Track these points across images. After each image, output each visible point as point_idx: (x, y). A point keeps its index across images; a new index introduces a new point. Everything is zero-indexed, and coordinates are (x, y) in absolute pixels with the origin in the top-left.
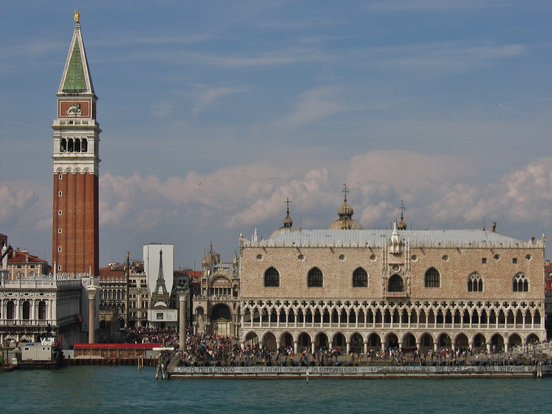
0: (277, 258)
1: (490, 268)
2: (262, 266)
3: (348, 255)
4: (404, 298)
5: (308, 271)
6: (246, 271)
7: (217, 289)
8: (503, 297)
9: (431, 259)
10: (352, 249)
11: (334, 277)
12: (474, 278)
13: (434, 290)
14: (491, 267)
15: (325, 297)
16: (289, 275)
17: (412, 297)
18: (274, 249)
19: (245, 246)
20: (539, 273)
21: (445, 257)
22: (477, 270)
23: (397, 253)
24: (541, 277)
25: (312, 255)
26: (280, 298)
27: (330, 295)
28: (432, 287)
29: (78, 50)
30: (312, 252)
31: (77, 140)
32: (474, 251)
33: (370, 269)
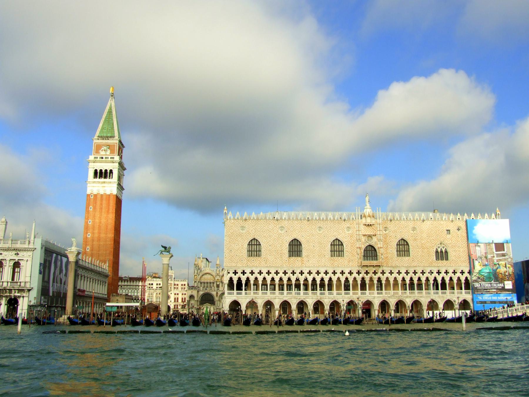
0: (259, 230)
1: (453, 239)
2: (245, 237)
4: (379, 266)
5: (287, 242)
6: (230, 242)
7: (204, 283)
9: (401, 230)
10: (329, 221)
13: (405, 259)
16: (270, 246)
17: (385, 265)
18: (256, 222)
19: (228, 218)
21: (414, 229)
23: (371, 225)
25: (292, 227)
26: (262, 267)
30: (292, 224)
31: (106, 170)
33: (346, 240)
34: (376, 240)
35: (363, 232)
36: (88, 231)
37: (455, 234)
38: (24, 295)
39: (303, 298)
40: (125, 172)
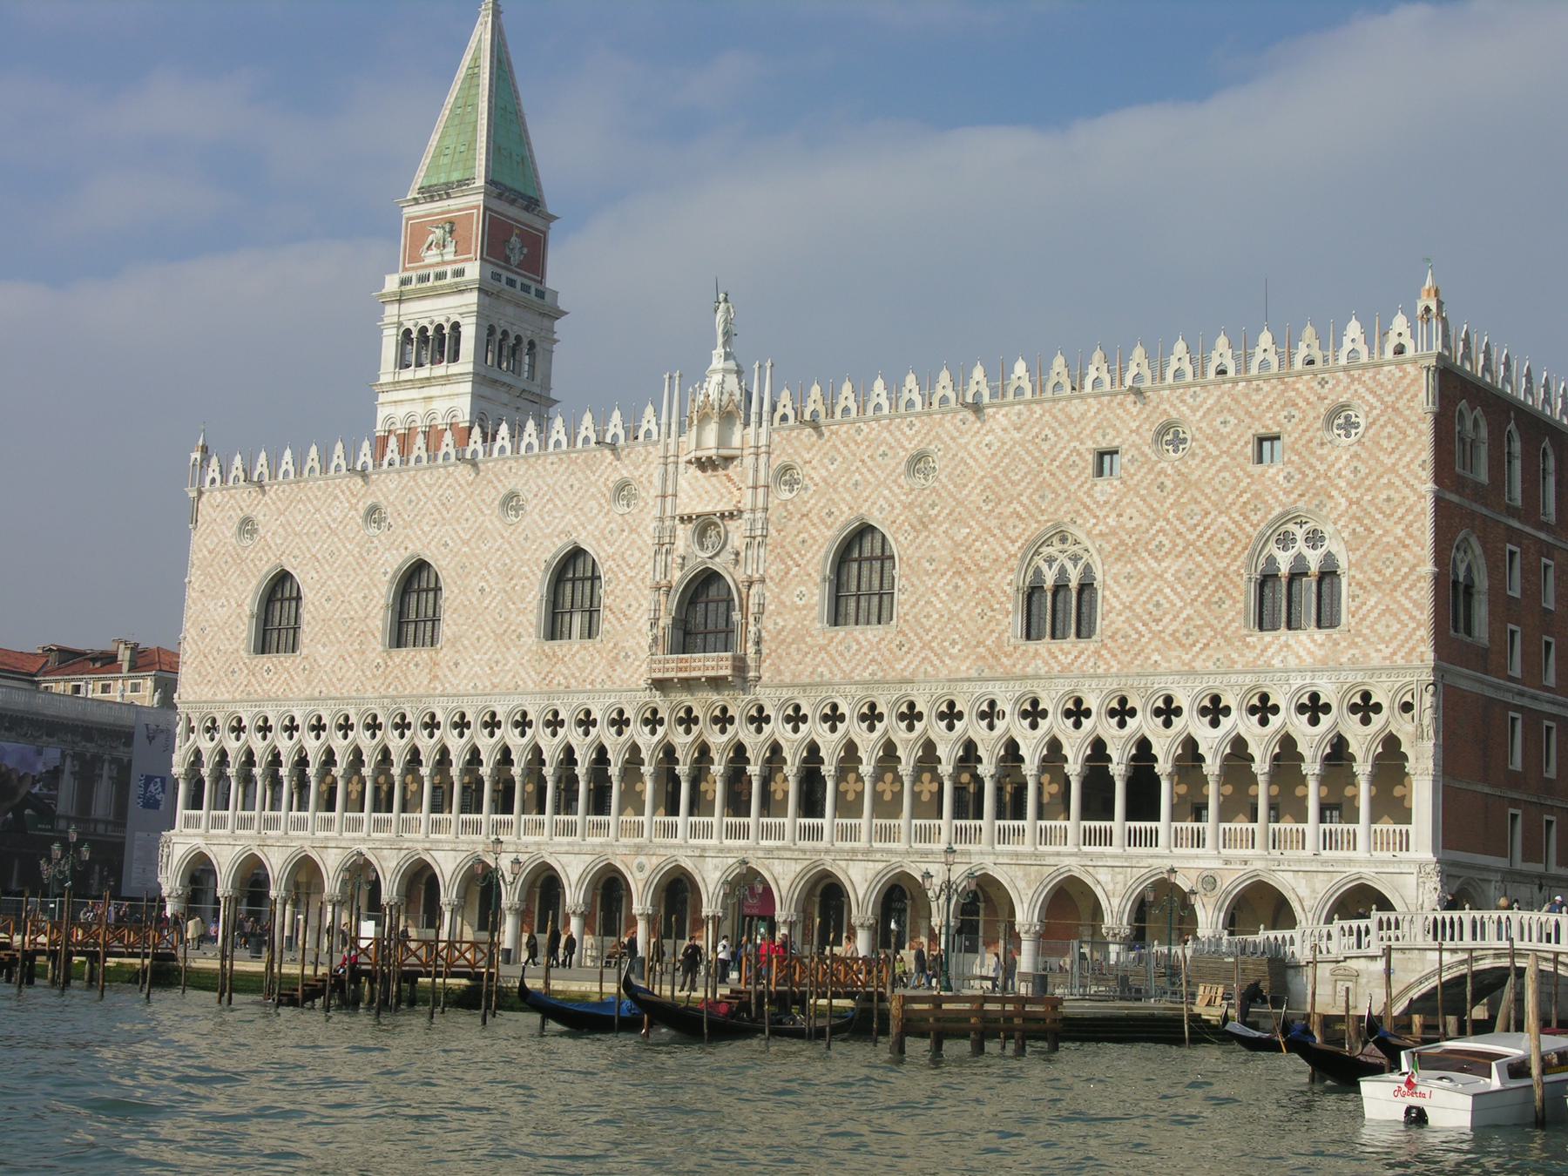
1: (1131, 503)
3: (536, 489)
5: (388, 577)
8: (1198, 665)
9: (857, 477)
11: (478, 599)
12: (1055, 566)
13: (861, 638)
14: (1137, 494)
16: (328, 599)
20: (1401, 511)
22: (1067, 520)
24: (1410, 536)
27: (456, 682)
28: (868, 623)
30: (412, 489)
31: (440, 328)
32: (1055, 417)
33: (611, 551)
34: (737, 544)
37: (1144, 470)
39: (419, 846)
40: (558, 324)
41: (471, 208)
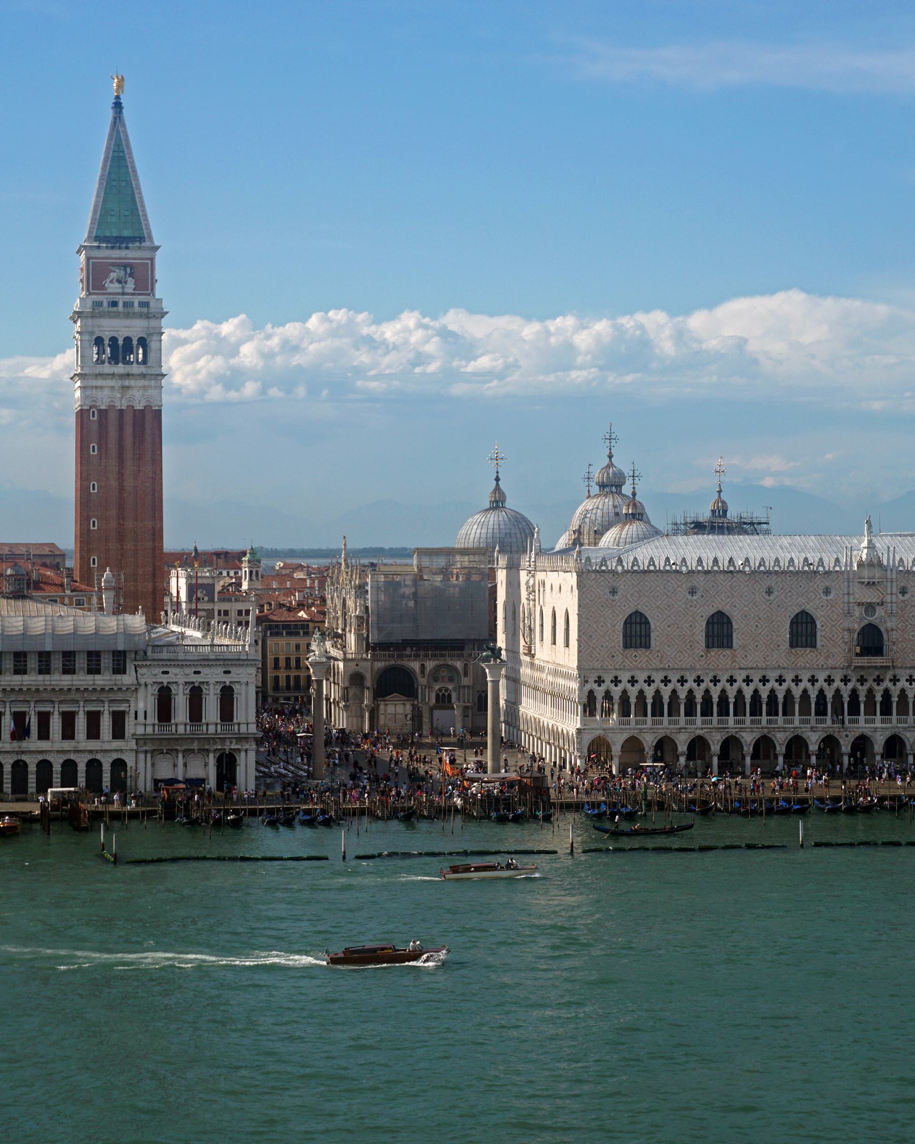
4: (887, 668)
10: (788, 575)
15: (738, 666)
16: (669, 626)
23: (874, 583)
25: (713, 586)
26: (653, 669)
29: (121, 154)
31: (128, 340)
33: (822, 614)
34: (883, 614)
35: (857, 596)
36: (91, 514)
38: (247, 747)
41: (148, 259)
